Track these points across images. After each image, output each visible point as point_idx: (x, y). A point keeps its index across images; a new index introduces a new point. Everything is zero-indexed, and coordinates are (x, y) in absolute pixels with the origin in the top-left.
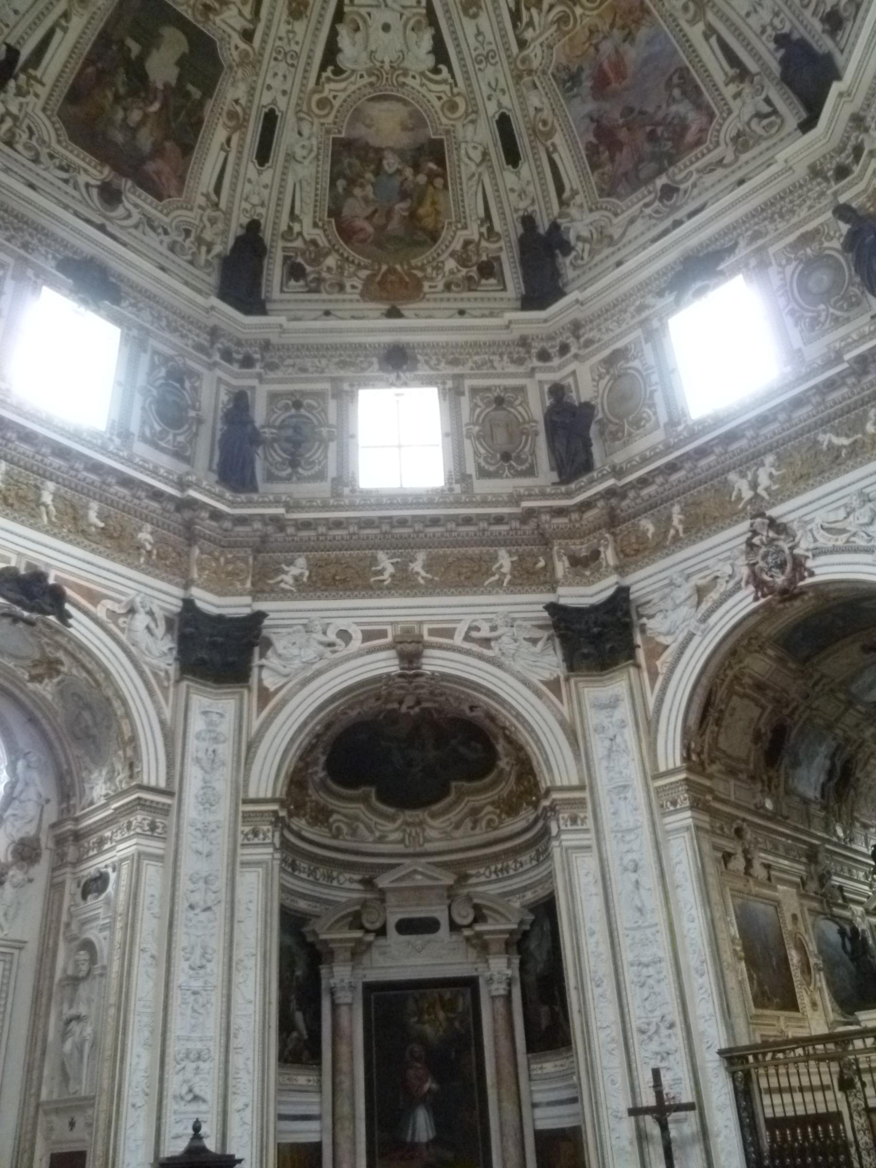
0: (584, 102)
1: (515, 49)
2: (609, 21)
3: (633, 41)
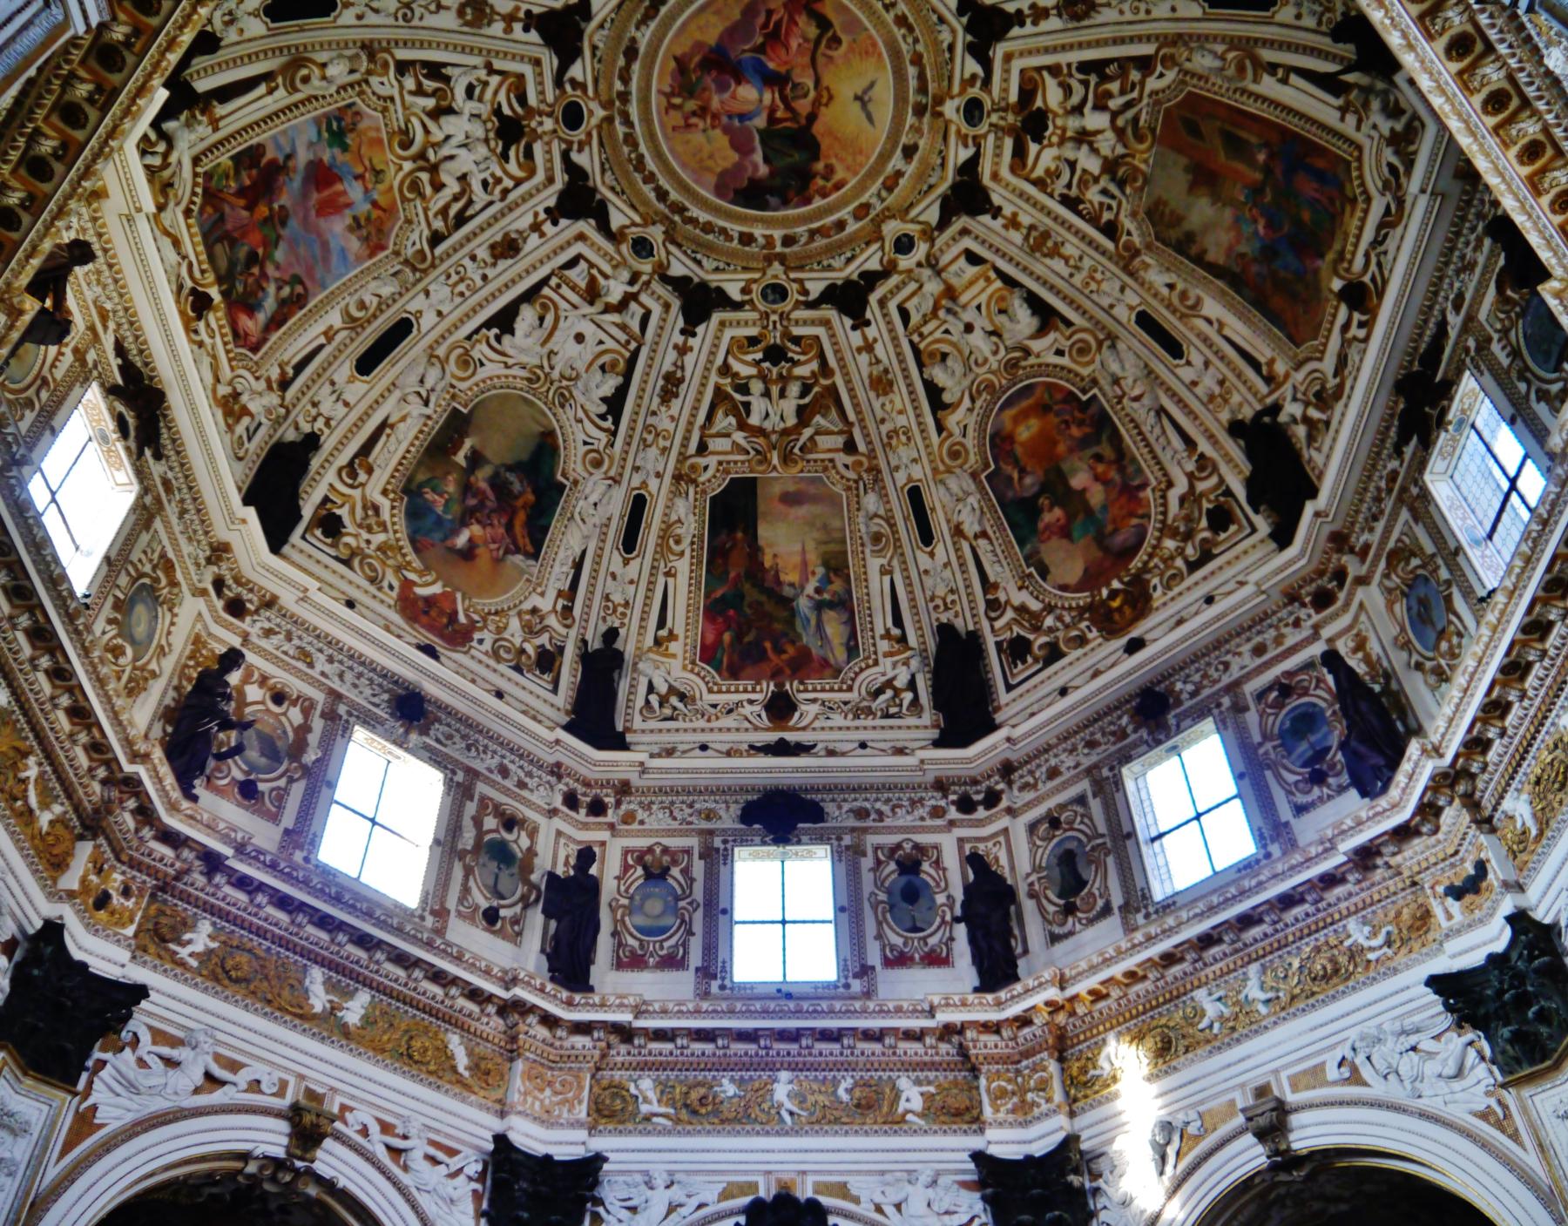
0: (311, 145)
1: (403, 54)
2: (382, 201)
3: (350, 229)
